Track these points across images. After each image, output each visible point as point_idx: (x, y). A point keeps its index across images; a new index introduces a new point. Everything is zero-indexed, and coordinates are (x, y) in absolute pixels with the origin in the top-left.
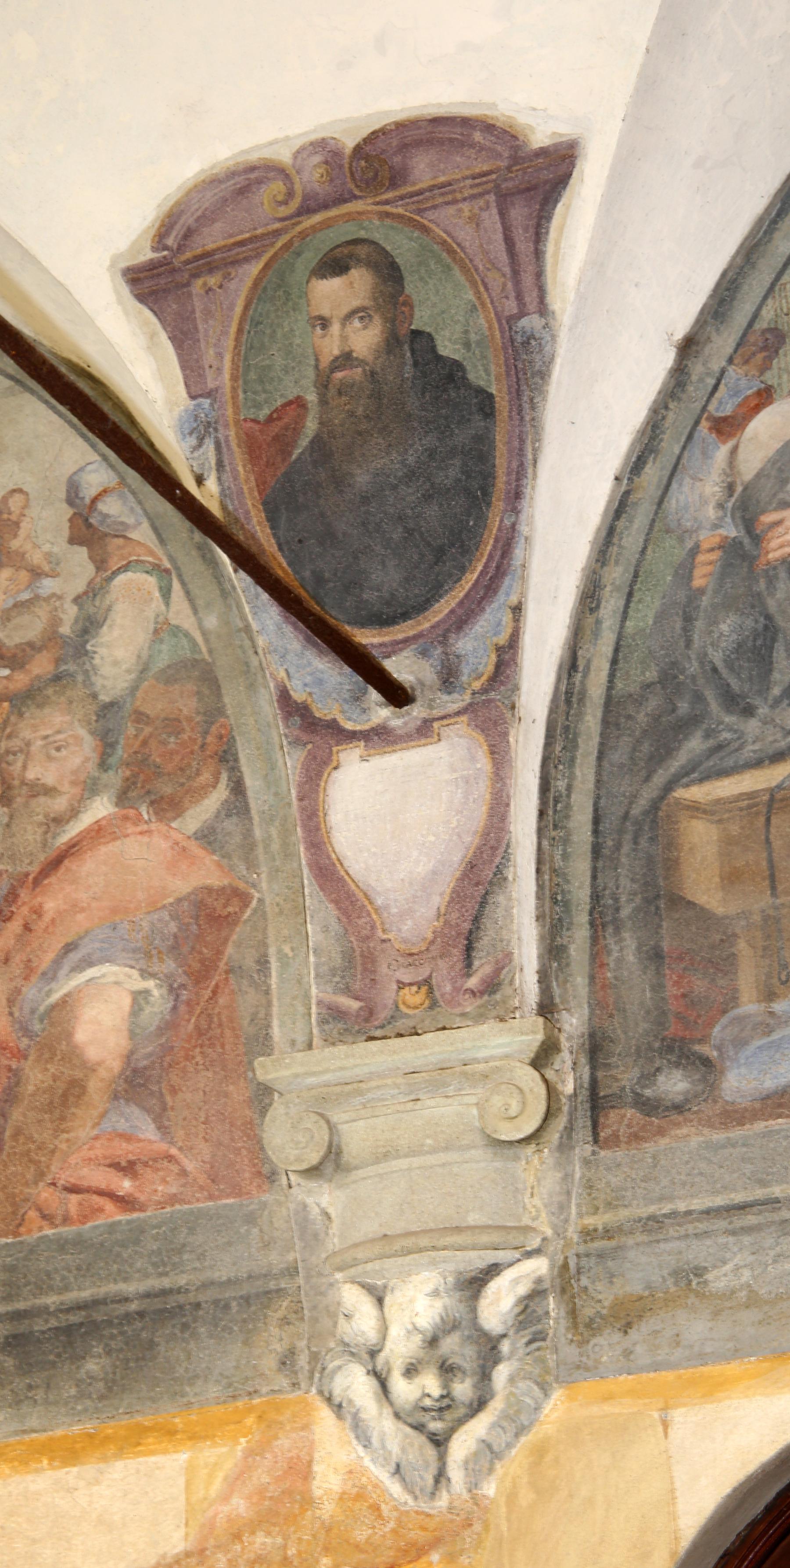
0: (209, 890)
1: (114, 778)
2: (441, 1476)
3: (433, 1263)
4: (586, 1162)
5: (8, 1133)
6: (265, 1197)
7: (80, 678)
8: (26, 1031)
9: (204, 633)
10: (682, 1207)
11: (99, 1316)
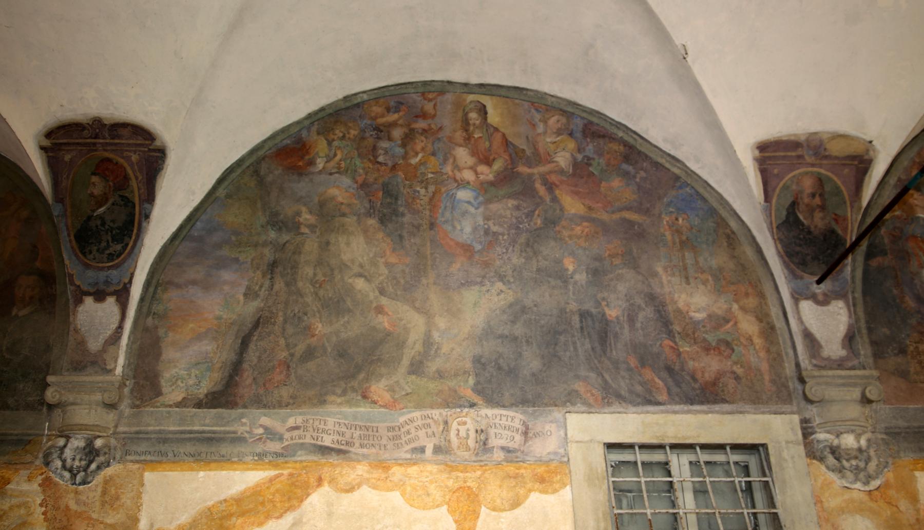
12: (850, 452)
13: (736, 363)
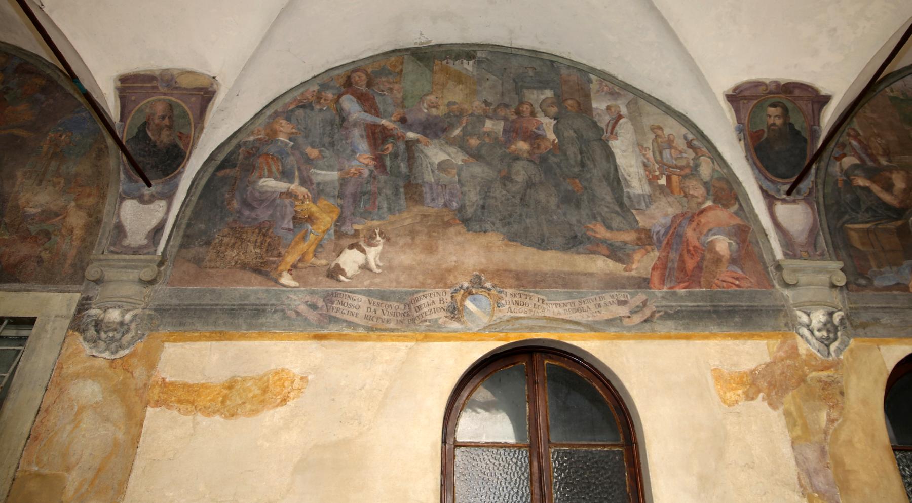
0: (740, 225)
1: (712, 197)
2: (829, 353)
3: (824, 308)
4: (847, 294)
5: (704, 267)
8: (704, 246)
10: (871, 306)
11: (736, 309)
12: (110, 325)
13: (46, 249)
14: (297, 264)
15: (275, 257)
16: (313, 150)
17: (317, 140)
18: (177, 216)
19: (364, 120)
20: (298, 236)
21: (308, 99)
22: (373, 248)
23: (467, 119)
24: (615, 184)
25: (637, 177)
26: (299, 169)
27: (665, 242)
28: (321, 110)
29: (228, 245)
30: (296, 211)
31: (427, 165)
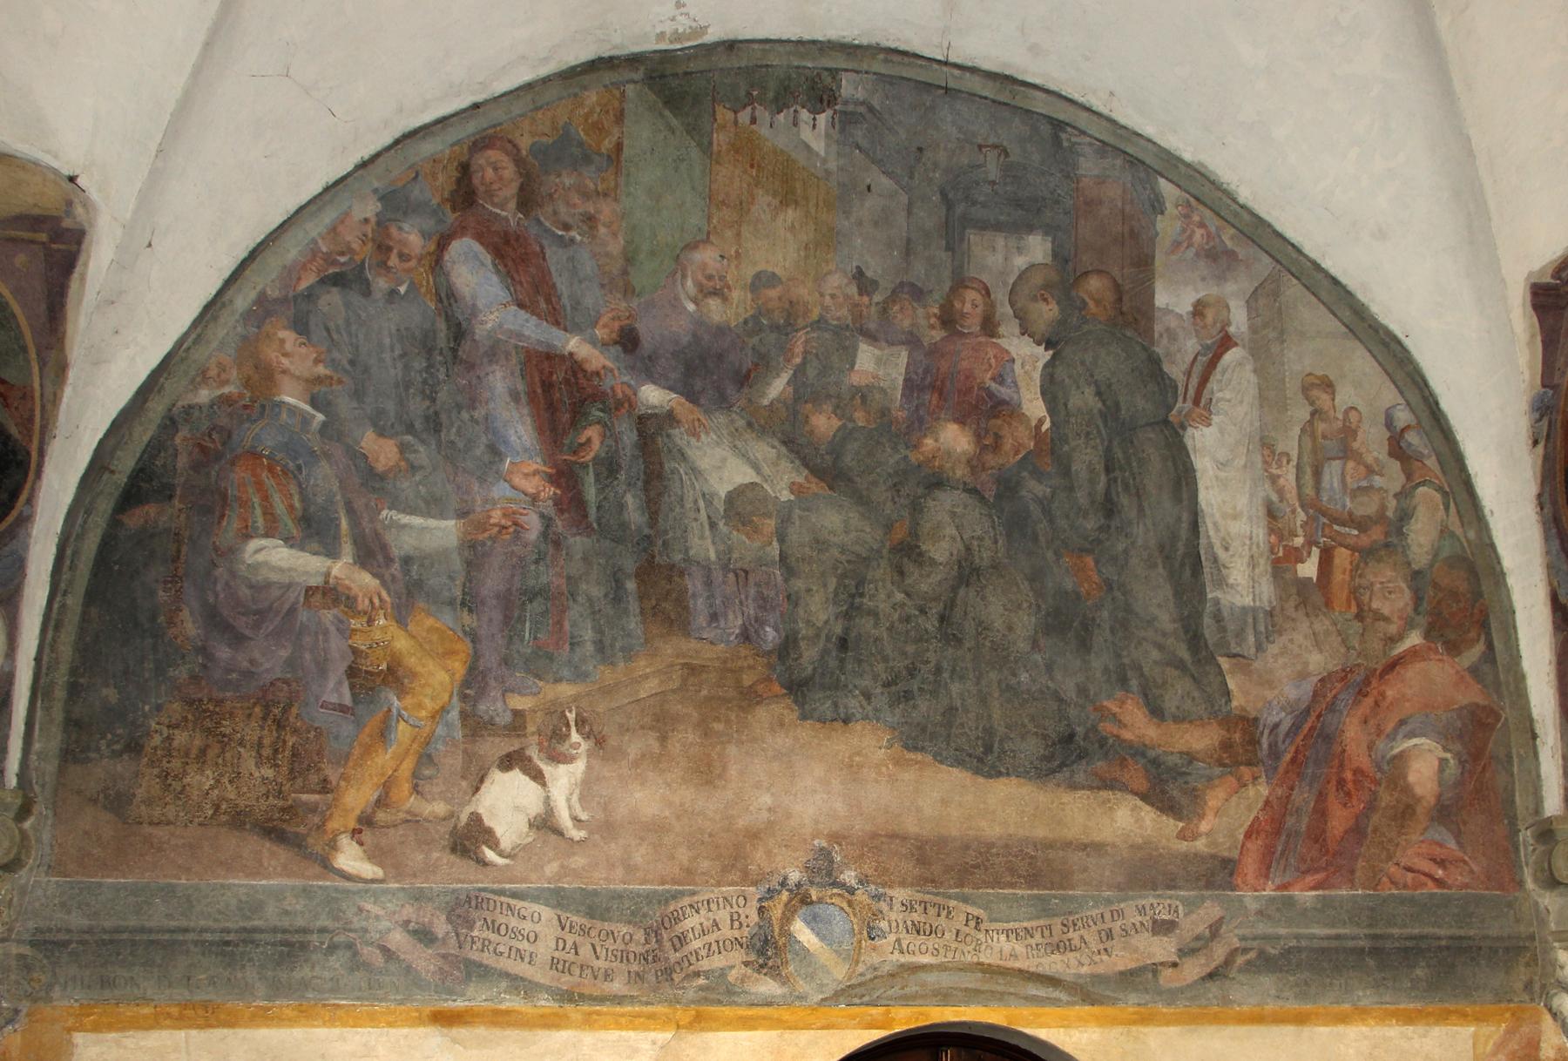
0: (1477, 705)
1: (1423, 620)
5: (1370, 829)
6: (1517, 894)
7: (1400, 550)
8: (1380, 769)
9: (1468, 541)
14: (374, 812)
15: (313, 792)
16: (382, 441)
17: (390, 406)
18: (38, 659)
19: (520, 336)
20: (367, 730)
21: (351, 251)
22: (562, 768)
23: (806, 341)
24: (1188, 572)
25: (1246, 553)
26: (351, 511)
27: (1288, 757)
28: (393, 293)
29: (187, 755)
30: (355, 652)
31: (696, 502)
